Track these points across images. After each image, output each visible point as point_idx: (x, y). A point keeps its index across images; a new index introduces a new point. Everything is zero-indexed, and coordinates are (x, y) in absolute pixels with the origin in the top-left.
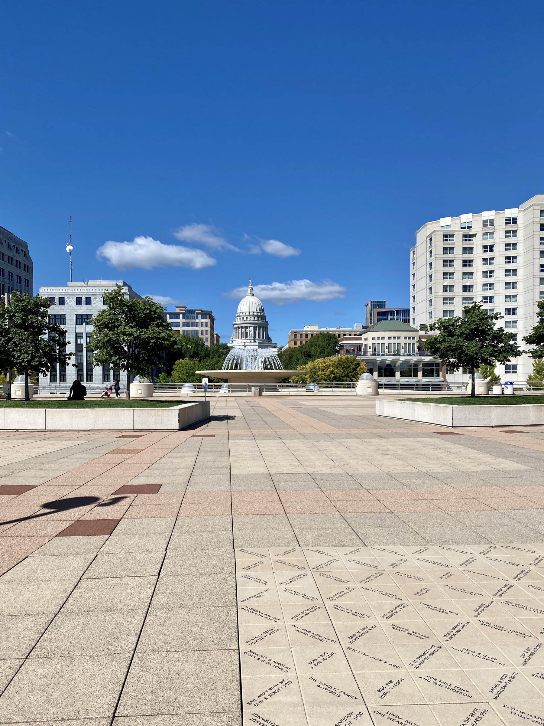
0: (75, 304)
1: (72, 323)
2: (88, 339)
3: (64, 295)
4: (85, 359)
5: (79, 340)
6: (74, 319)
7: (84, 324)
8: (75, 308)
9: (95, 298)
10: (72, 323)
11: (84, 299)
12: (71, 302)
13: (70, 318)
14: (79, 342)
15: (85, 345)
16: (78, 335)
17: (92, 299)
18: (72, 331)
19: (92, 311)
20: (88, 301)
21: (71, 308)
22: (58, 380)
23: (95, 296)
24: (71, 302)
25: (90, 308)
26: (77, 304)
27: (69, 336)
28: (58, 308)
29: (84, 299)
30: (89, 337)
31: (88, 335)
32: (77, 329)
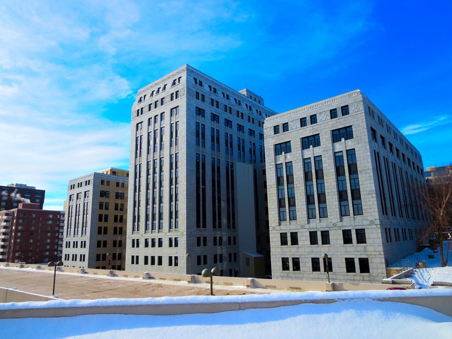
4: (315, 189)
8: (300, 131)
12: (295, 125)
20: (314, 119)
26: (301, 126)
28: (282, 136)
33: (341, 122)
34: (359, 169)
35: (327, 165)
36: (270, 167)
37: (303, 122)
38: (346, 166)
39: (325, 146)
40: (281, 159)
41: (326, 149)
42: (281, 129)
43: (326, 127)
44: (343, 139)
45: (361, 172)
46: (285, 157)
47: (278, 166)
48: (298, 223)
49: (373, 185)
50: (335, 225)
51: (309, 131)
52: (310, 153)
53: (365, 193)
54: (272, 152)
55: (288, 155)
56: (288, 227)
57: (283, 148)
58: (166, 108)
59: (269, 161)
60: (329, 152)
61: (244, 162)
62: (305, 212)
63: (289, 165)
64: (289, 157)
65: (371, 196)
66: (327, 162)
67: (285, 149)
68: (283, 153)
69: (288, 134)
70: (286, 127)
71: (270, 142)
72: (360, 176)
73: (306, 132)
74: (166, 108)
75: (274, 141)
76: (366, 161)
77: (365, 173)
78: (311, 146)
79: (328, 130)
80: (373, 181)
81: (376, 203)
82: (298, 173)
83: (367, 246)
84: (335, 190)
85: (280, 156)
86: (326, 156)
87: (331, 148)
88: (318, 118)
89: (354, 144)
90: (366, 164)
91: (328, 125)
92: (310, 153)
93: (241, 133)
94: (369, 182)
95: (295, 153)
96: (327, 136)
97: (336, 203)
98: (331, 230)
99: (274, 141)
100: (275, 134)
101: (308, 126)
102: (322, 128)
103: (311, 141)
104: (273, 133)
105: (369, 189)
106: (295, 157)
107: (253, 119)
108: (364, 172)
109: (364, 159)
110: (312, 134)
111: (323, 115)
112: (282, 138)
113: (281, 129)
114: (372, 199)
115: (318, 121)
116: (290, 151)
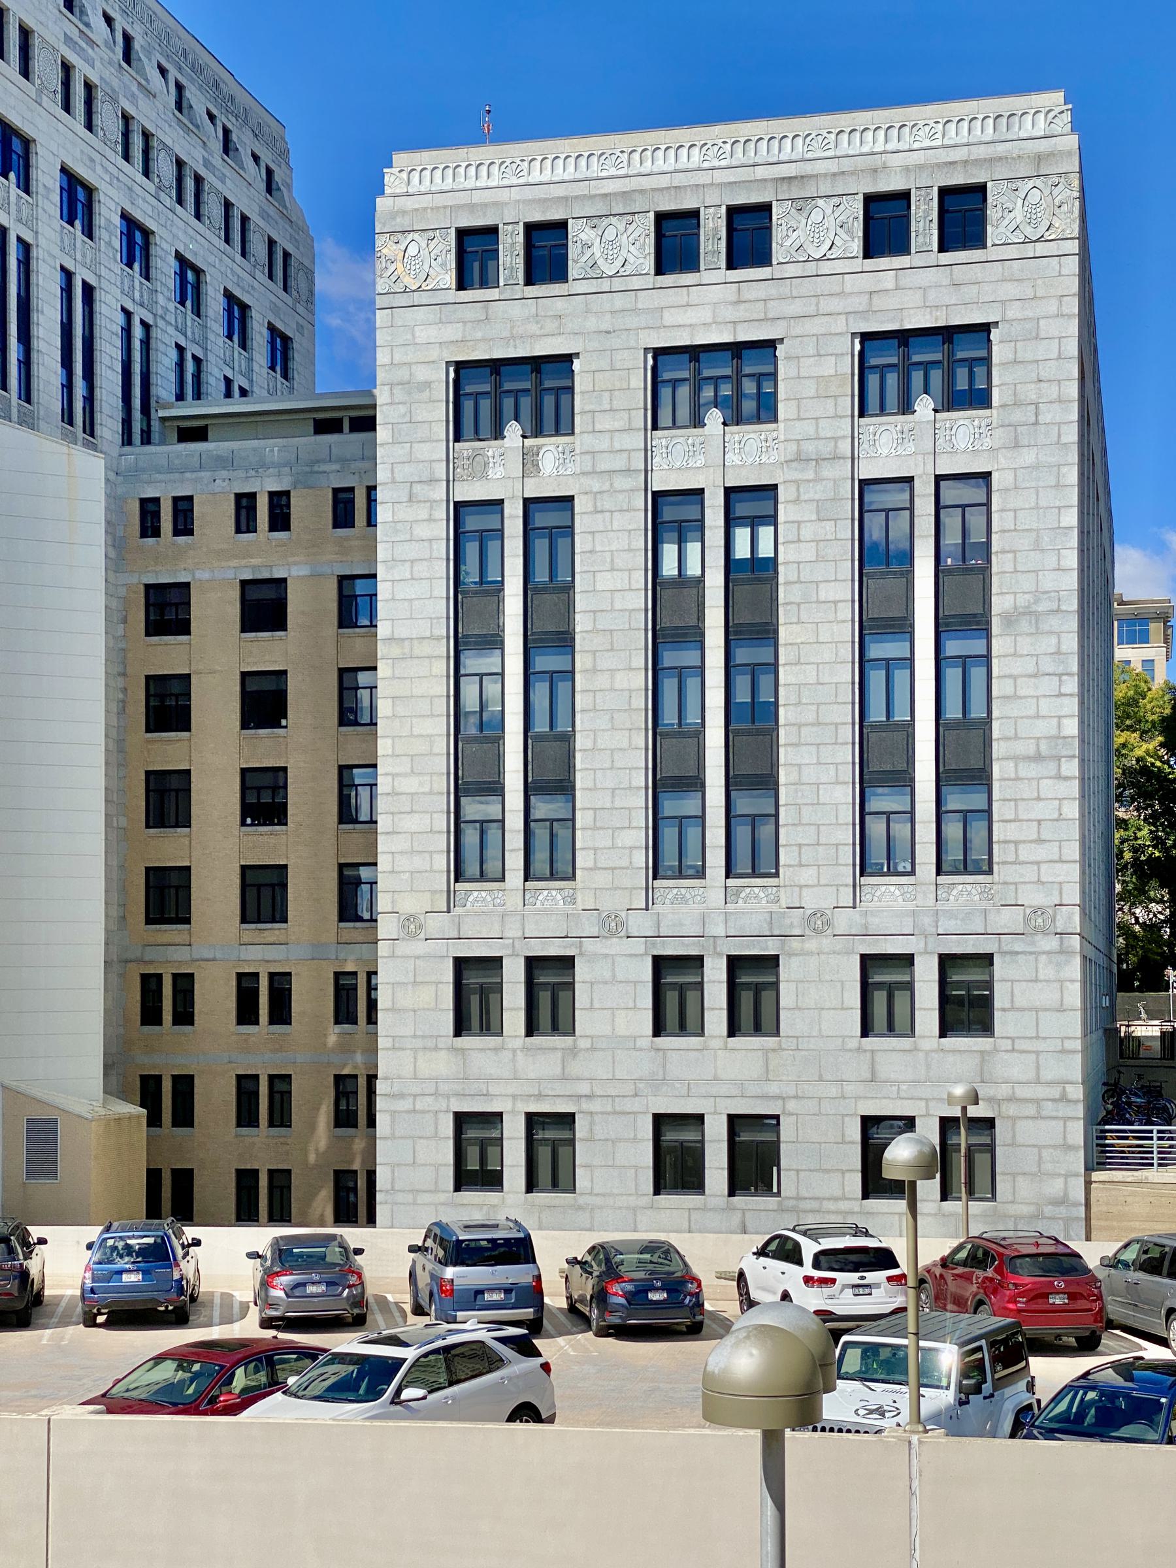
0: (649, 264)
3: (566, 200)
5: (669, 552)
6: (638, 381)
7: (714, 417)
9: (802, 204)
14: (669, 568)
15: (715, 581)
18: (621, 483)
19: (775, 309)
20: (749, 235)
22: (515, 861)
23: (803, 190)
27: (598, 523)
30: (754, 523)
31: (741, 509)
33: (922, 290)
34: (999, 604)
35: (807, 552)
36: (406, 513)
38: (923, 568)
39: (808, 428)
41: (809, 448)
43: (827, 305)
44: (924, 406)
45: (1009, 619)
47: (472, 522)
48: (584, 900)
49: (1072, 706)
50: (817, 922)
51: (710, 306)
52: (700, 461)
53: (1020, 748)
54: (435, 412)
55: (550, 448)
56: (511, 919)
57: (514, 392)
59: (405, 472)
60: (828, 471)
61: (28, 422)
62: (637, 836)
64: (555, 466)
65: (1050, 768)
66: (807, 532)
67: (526, 403)
68: (513, 430)
69: (560, 304)
71: (416, 335)
72: (999, 645)
75: (452, 332)
76: (1051, 561)
77: (1038, 632)
78: (714, 417)
79: (840, 325)
80: (1072, 685)
81: (1072, 810)
82: (605, 582)
83: (996, 1050)
84: (842, 712)
86: (809, 493)
87: (845, 447)
88: (778, 234)
89: (988, 442)
90: (1049, 582)
91: (841, 294)
92: (700, 461)
93: (14, 191)
94: (1048, 685)
95: (603, 443)
96: (828, 367)
97: (842, 796)
98: (790, 955)
99: (452, 332)
100: (461, 285)
101: (706, 276)
103: (725, 378)
104: (450, 279)
105: (1044, 728)
106: (604, 462)
107: (89, 87)
108: (1024, 625)
109: (1037, 547)
111: (816, 216)
112: (516, 320)
114: (1049, 787)
115: (778, 254)
116: (562, 425)
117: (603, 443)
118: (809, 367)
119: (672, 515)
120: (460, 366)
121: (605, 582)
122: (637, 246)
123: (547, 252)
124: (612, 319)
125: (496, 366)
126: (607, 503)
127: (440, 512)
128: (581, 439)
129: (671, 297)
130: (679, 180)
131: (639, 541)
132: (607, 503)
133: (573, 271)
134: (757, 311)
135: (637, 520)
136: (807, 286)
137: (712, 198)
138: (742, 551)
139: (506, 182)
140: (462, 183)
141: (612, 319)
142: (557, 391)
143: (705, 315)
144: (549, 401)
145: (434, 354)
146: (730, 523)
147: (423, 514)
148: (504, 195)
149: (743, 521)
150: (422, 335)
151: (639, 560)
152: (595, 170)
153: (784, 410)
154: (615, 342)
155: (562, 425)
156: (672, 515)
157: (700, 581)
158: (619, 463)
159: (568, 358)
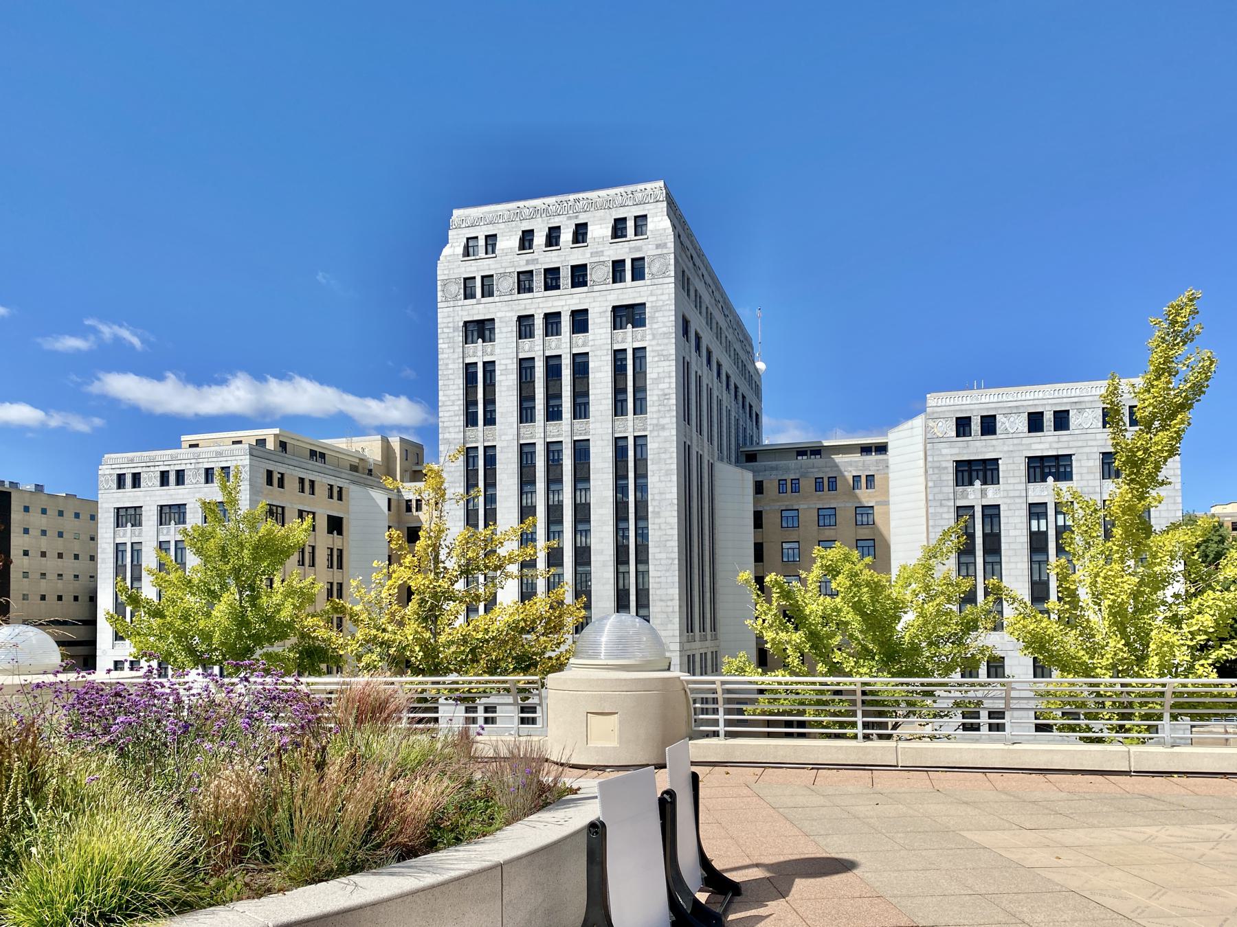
1: (1017, 480)
2: (1060, 518)
5: (1034, 523)
6: (1023, 467)
7: (1050, 479)
8: (1025, 441)
10: (1017, 480)
11: (1048, 419)
12: (1013, 424)
13: (1011, 467)
16: (987, 512)
17: (1071, 413)
18: (1018, 500)
20: (1062, 420)
21: (1016, 441)
24: (1013, 424)
25: (1065, 438)
28: (978, 443)
29: (1048, 419)
32: (1030, 493)
37: (1035, 422)
39: (1084, 483)
40: (971, 497)
42: (976, 426)
46: (983, 494)
51: (1048, 443)
55: (991, 489)
58: (599, 300)
63: (992, 513)
64: (993, 495)
67: (981, 474)
68: (978, 483)
70: (989, 425)
73: (1041, 446)
74: (599, 300)
78: (1050, 479)
85: (969, 489)
87: (1098, 489)
95: (1011, 487)
99: (955, 451)
100: (958, 436)
101: (1045, 433)
102: (1080, 444)
104: (954, 434)
110: (1054, 453)
113: (976, 426)
117: (1011, 487)
118: (1085, 463)
119: (1036, 511)
120: (957, 462)
121: (1012, 533)
122: (1022, 423)
123: (989, 425)
124: (1012, 447)
125: (970, 462)
126: (1012, 507)
127: (952, 510)
128: (1001, 486)
129: (1034, 440)
130: (1036, 402)
131: (1025, 519)
132: (1012, 507)
133: (998, 431)
134: (1065, 445)
135: (1024, 512)
136: (1083, 437)
137: (1048, 408)
138: (1061, 523)
139: (975, 402)
140: (956, 402)
141: (1012, 447)
142: (992, 470)
143: (1047, 446)
144: (989, 473)
145: (949, 458)
146: (1057, 513)
147: (945, 509)
148: (972, 407)
149: (1061, 513)
150: (945, 451)
151: (1025, 526)
152: (1005, 398)
153: (1074, 477)
154: (1014, 454)
155: (995, 480)
156: (1036, 511)
157: (1045, 533)
158: (1017, 494)
159: (997, 460)
